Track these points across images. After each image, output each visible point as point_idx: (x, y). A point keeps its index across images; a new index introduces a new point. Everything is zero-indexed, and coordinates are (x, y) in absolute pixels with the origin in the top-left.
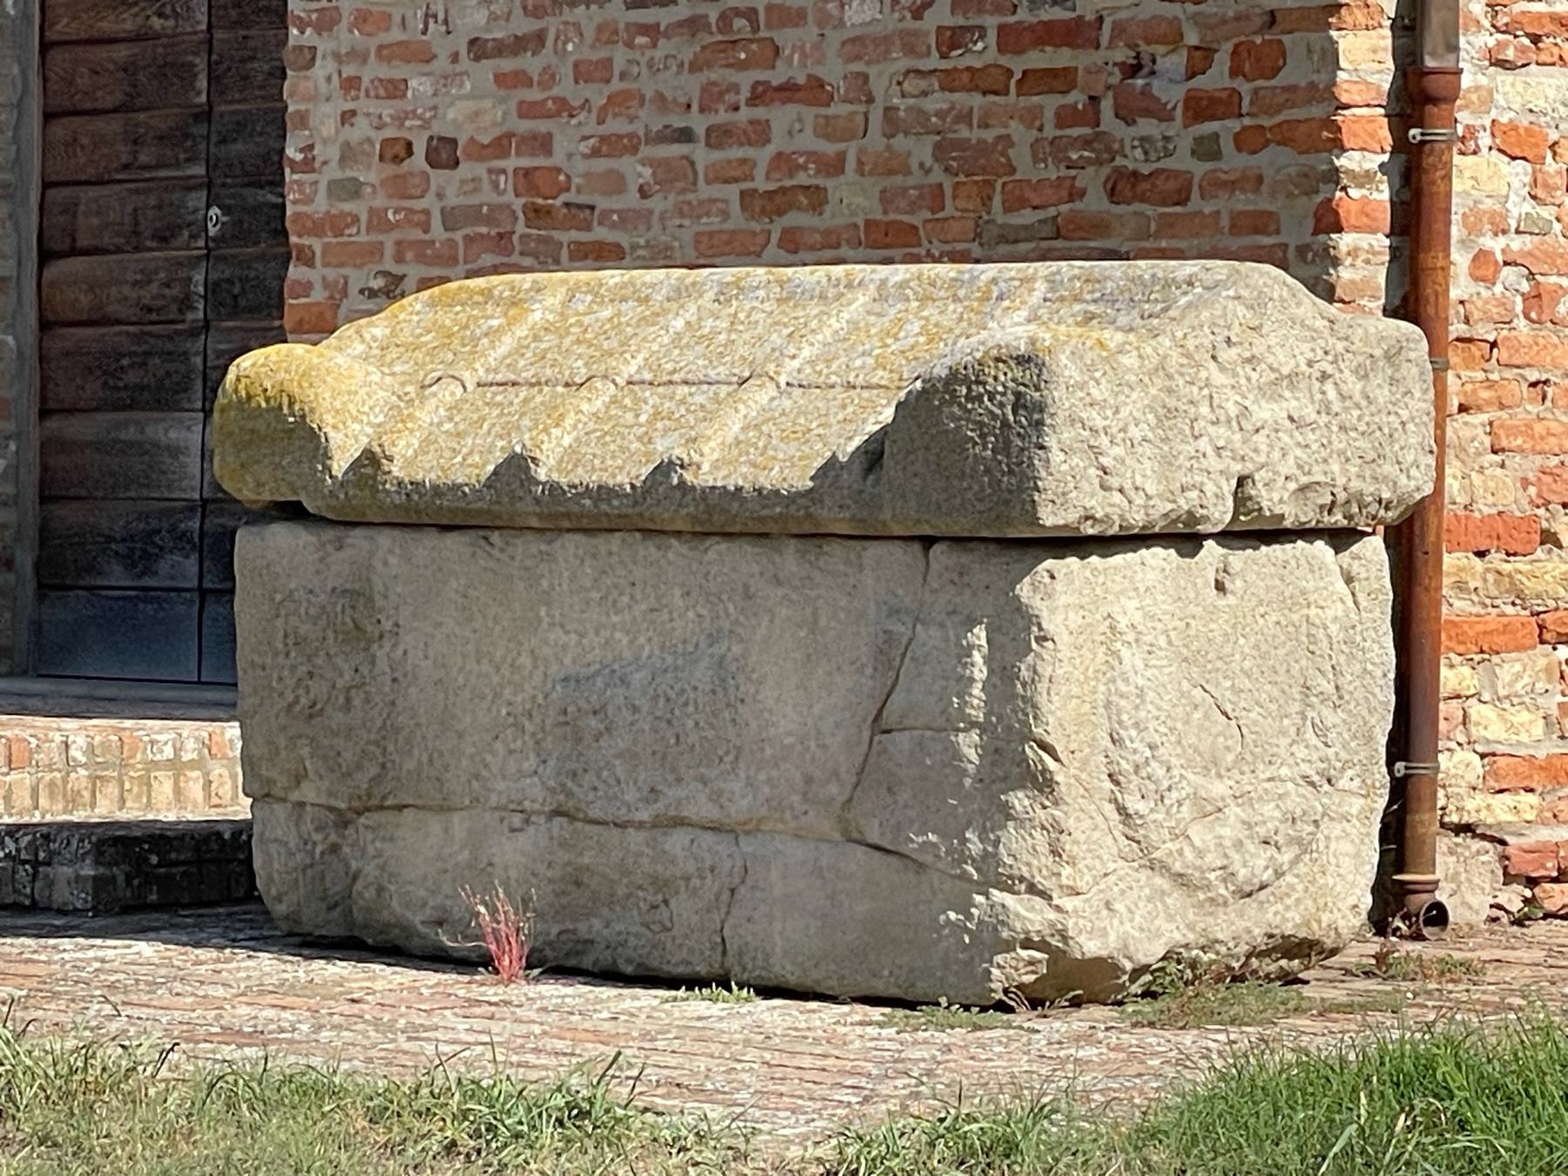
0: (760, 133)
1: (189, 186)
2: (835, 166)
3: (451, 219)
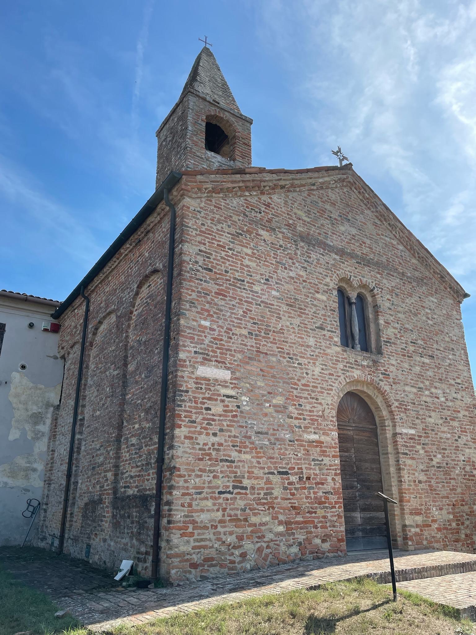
0: (450, 483)
1: (354, 481)
3: (422, 490)
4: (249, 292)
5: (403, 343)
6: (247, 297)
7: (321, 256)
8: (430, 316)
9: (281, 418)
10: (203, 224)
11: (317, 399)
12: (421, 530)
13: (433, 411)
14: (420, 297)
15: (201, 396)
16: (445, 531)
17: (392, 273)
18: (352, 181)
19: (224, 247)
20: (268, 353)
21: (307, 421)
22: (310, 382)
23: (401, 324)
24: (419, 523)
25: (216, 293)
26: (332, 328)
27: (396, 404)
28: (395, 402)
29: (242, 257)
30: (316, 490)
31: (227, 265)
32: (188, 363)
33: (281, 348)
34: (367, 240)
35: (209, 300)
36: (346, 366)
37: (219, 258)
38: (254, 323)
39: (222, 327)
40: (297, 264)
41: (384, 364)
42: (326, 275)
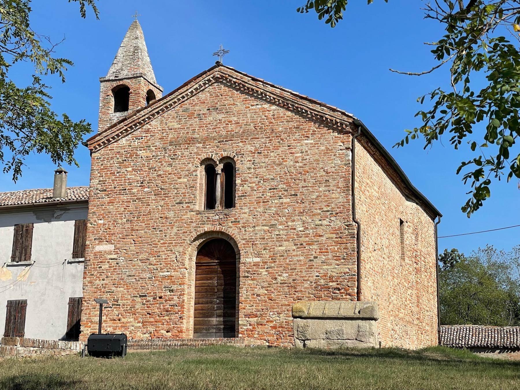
4: (129, 195)
5: (260, 192)
6: (127, 199)
7: (186, 150)
8: (300, 160)
9: (144, 266)
10: (102, 165)
11: (171, 251)
12: (253, 328)
13: (285, 241)
14: (288, 146)
15: (97, 261)
16: (280, 329)
17: (257, 136)
18: (219, 76)
19: (114, 173)
20: (139, 229)
21: (161, 266)
22: (167, 241)
23: (260, 177)
24: (252, 323)
25: (108, 203)
26: (190, 200)
27: (244, 242)
28: (242, 241)
29: (126, 175)
30: (165, 304)
31: (115, 183)
32: (90, 246)
33: (148, 224)
34: (233, 118)
35: (103, 208)
36: (198, 224)
37: (110, 181)
38: (131, 214)
39: (110, 222)
40: (165, 164)
41: (235, 214)
42: (188, 163)
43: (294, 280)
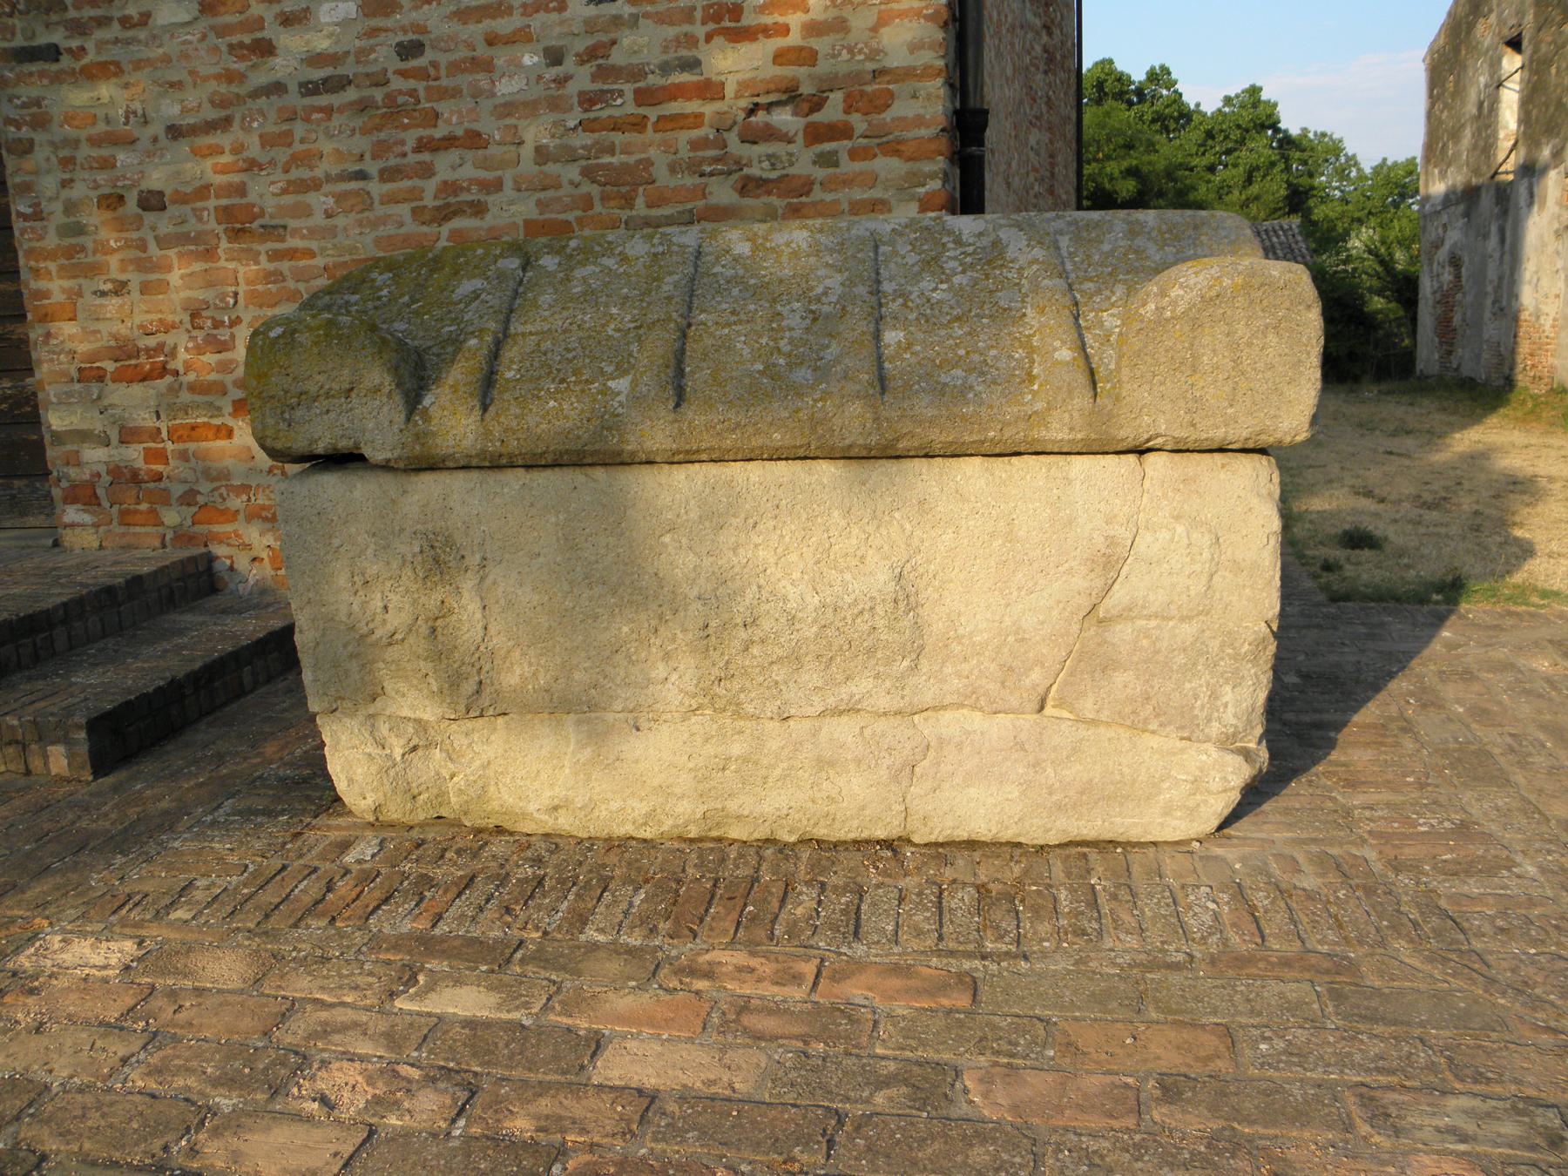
0: (427, 171)
2: (498, 185)
43: (410, 50)
